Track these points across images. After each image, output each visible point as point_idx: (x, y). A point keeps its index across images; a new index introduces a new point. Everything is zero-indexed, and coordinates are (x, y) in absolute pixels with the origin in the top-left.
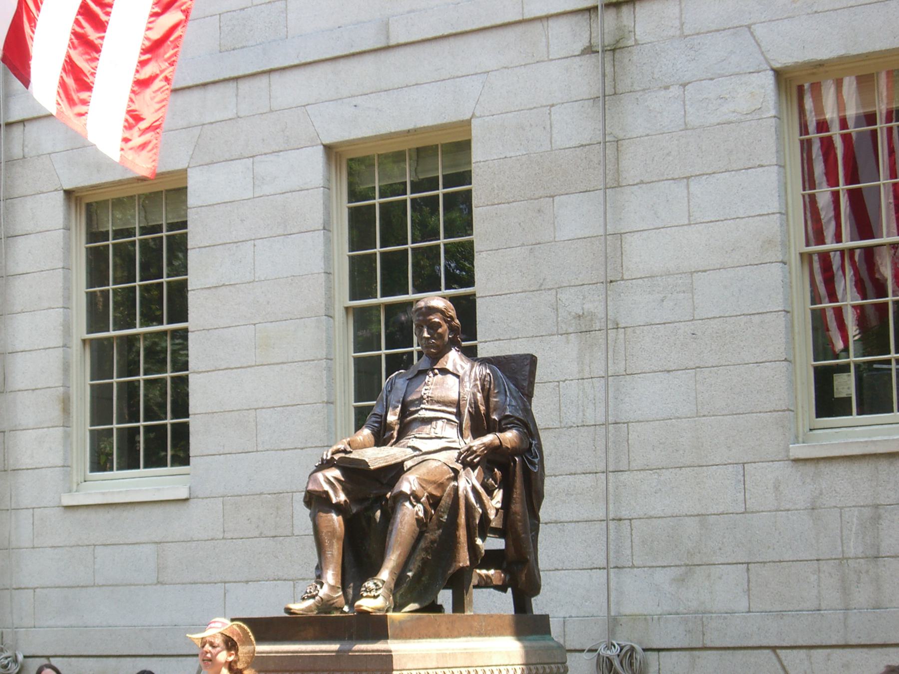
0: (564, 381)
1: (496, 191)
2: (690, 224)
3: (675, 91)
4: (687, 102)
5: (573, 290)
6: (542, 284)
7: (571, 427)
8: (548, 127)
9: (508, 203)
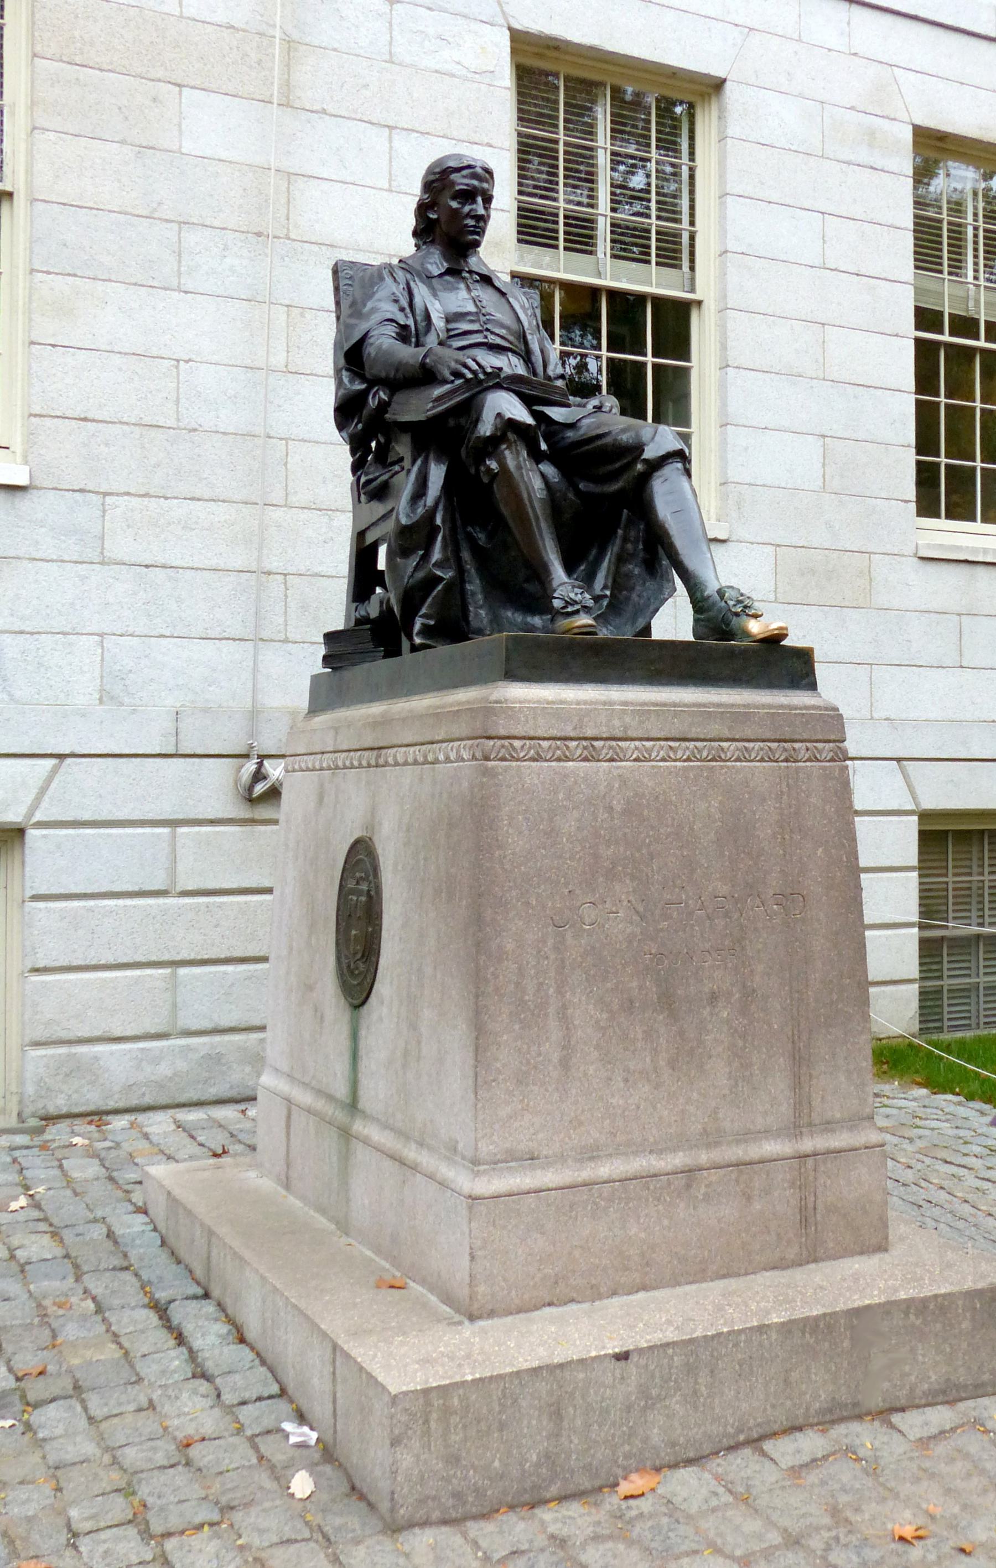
0: (187, 362)
6: (155, 210)
7: (195, 430)
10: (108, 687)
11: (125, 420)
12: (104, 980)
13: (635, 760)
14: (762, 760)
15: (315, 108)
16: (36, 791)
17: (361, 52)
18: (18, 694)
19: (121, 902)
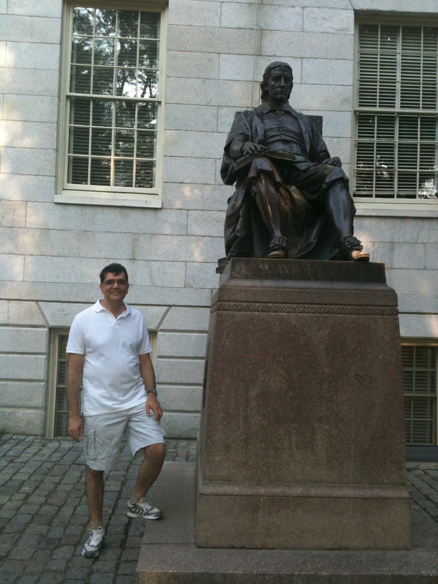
1: (183, 44)
2: (301, 84)
3: (298, 9)
4: (305, 17)
5: (228, 109)
6: (209, 102)
8: (219, 13)
9: (190, 52)
10: (187, 281)
11: (196, 182)
12: (182, 389)
13: (287, 312)
14: (351, 314)
15: (271, 55)
16: (161, 318)
17: (291, 30)
18: (156, 283)
19: (189, 360)
